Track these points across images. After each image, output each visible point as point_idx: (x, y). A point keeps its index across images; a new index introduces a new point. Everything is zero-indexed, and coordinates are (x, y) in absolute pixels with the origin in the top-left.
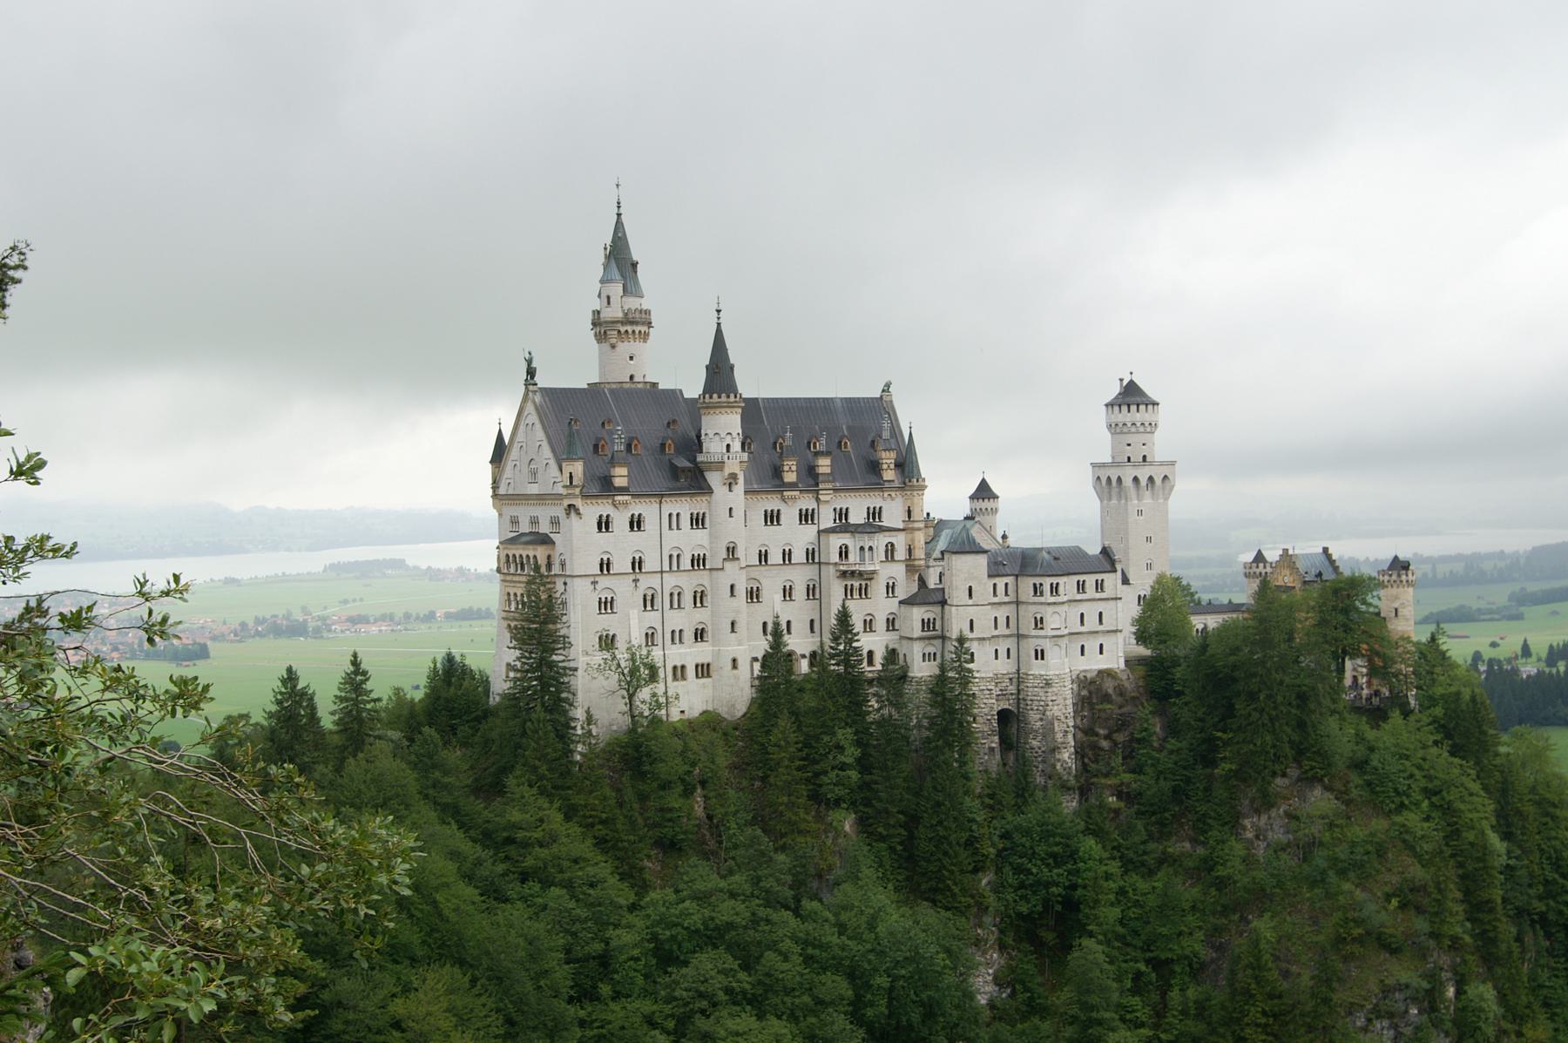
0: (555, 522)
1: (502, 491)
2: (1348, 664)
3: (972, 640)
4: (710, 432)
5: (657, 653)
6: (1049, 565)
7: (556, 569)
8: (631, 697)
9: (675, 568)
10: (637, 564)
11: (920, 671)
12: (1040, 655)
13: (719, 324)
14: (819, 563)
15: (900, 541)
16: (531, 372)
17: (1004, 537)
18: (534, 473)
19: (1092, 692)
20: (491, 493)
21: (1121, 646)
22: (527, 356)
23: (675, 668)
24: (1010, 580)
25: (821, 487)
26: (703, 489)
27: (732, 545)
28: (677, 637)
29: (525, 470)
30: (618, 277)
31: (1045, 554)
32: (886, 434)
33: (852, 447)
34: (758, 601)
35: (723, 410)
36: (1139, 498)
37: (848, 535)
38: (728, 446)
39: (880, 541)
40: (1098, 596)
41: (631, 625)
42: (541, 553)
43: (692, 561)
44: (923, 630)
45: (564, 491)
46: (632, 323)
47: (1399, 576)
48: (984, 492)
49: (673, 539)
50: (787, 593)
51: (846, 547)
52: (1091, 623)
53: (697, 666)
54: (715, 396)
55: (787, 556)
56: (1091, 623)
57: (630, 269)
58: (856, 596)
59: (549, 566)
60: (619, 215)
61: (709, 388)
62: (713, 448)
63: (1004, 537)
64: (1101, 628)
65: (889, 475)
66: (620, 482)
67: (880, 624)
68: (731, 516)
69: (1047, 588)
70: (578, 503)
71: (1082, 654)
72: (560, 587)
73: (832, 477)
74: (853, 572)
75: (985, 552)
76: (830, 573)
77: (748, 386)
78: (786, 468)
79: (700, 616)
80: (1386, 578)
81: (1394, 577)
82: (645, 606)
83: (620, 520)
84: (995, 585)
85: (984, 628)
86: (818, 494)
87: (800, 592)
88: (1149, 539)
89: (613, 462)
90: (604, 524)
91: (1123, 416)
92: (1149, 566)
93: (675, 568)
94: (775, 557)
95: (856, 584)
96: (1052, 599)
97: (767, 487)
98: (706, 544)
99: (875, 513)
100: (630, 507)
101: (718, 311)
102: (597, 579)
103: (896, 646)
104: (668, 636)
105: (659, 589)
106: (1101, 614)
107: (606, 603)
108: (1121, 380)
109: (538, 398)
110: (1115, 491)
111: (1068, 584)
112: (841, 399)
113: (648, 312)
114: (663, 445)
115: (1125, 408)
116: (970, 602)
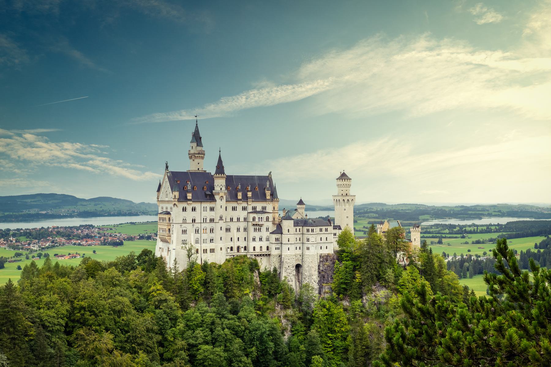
0: (171, 208)
1: (160, 200)
2: (398, 255)
3: (288, 244)
4: (216, 185)
5: (198, 246)
6: (311, 224)
7: (171, 222)
8: (189, 258)
9: (205, 222)
10: (194, 221)
11: (275, 252)
12: (308, 249)
13: (220, 155)
14: (248, 222)
15: (271, 216)
16: (167, 167)
17: (306, 215)
18: (167, 195)
19: (324, 259)
20: (157, 200)
21: (332, 247)
22: (166, 163)
23: (204, 250)
24: (301, 228)
25: (249, 200)
26: (215, 201)
27: (221, 216)
28: (205, 241)
29: (165, 194)
30: (195, 141)
31: (310, 221)
32: (268, 186)
33: (259, 189)
34: (230, 232)
35: (220, 178)
36: (345, 206)
37: (256, 214)
38: (221, 188)
39: (264, 216)
40: (326, 232)
41: (192, 237)
42: (167, 217)
43: (210, 220)
44: (276, 241)
45: (173, 200)
46: (199, 154)
47: (416, 229)
48: (301, 202)
49: (204, 214)
50: (238, 230)
51: (255, 217)
52: (324, 240)
53: (210, 249)
54: (218, 174)
55: (238, 219)
56: (324, 240)
57: (199, 139)
58: (257, 231)
59: (169, 220)
60: (197, 124)
61: (216, 173)
62: (217, 189)
63: (306, 215)
64: (327, 242)
65: (268, 197)
66: (189, 198)
67: (264, 239)
68: (221, 208)
69: (310, 230)
70: (177, 203)
71: (321, 249)
72: (172, 226)
73: (253, 197)
74: (256, 225)
75: (293, 219)
76: (250, 224)
77: (228, 171)
78: (238, 195)
79: (212, 235)
80: (412, 230)
81: (414, 230)
82: (196, 232)
83: (189, 208)
84: (296, 229)
85: (292, 240)
86: (247, 202)
87: (242, 229)
88: (347, 217)
89: (188, 191)
90: (184, 209)
91: (340, 182)
92: (347, 225)
93: (205, 222)
94: (235, 219)
95: (257, 228)
96: (312, 233)
97: (233, 200)
98: (214, 215)
99: (264, 208)
100: (192, 205)
101: (220, 151)
102: (182, 224)
103: (268, 245)
104: (202, 241)
105: (200, 227)
106: (327, 238)
107: (184, 231)
108: (341, 172)
109: (169, 174)
110: (338, 203)
111: (317, 229)
112: (257, 176)
113: (204, 151)
114: (203, 188)
115: (341, 180)
116: (289, 233)
